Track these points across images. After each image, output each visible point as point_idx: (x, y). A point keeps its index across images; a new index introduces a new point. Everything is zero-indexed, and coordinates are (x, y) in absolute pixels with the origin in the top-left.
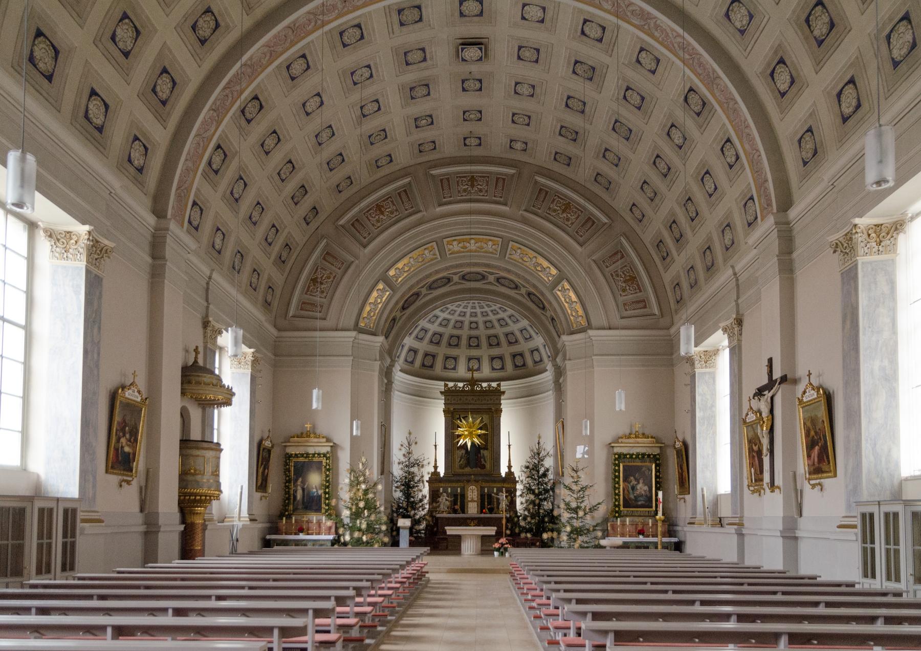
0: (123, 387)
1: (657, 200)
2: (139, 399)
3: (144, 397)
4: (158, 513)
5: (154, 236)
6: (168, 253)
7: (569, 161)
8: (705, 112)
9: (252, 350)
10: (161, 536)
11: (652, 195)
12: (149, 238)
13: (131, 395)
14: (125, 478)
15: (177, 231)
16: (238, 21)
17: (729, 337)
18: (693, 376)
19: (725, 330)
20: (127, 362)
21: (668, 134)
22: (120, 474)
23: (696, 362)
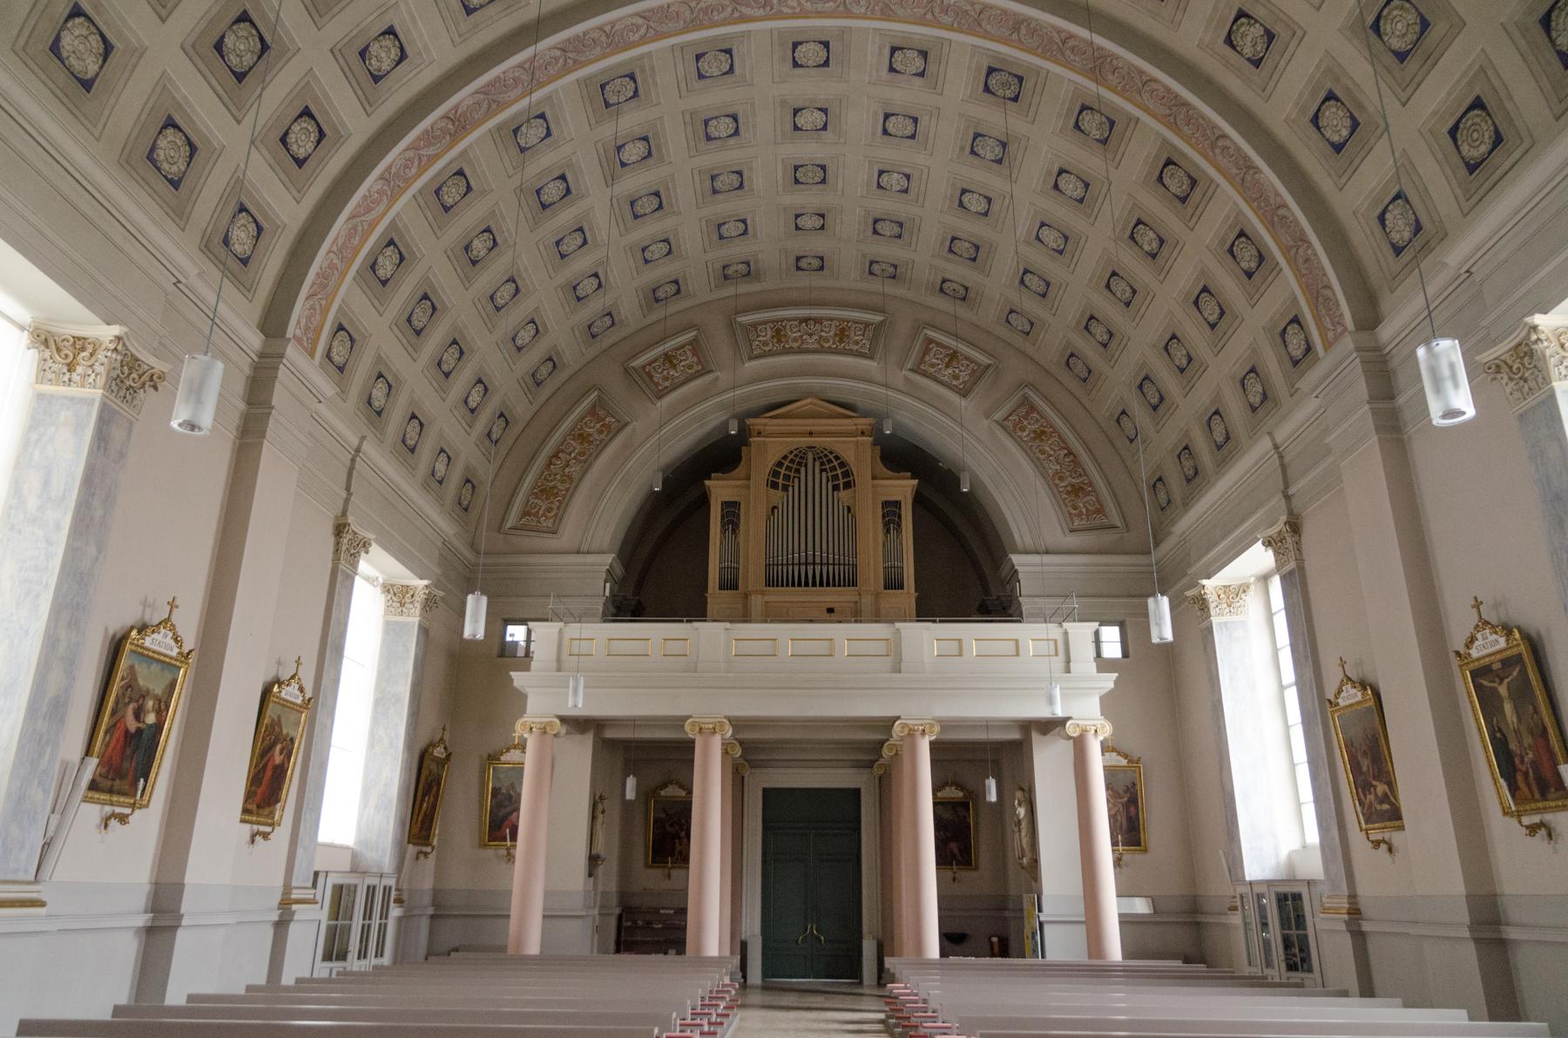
0: (143, 628)
1: (1113, 345)
2: (174, 653)
3: (308, 695)
4: (182, 885)
5: (256, 368)
6: (279, 397)
7: (964, 295)
8: (1196, 196)
9: (426, 582)
10: (181, 936)
11: (1106, 337)
12: (247, 371)
13: (290, 693)
14: (118, 810)
15: (301, 366)
16: (436, 44)
17: (1276, 553)
18: (1210, 630)
19: (1268, 543)
20: (163, 581)
21: (1132, 237)
22: (104, 804)
23: (1212, 606)
